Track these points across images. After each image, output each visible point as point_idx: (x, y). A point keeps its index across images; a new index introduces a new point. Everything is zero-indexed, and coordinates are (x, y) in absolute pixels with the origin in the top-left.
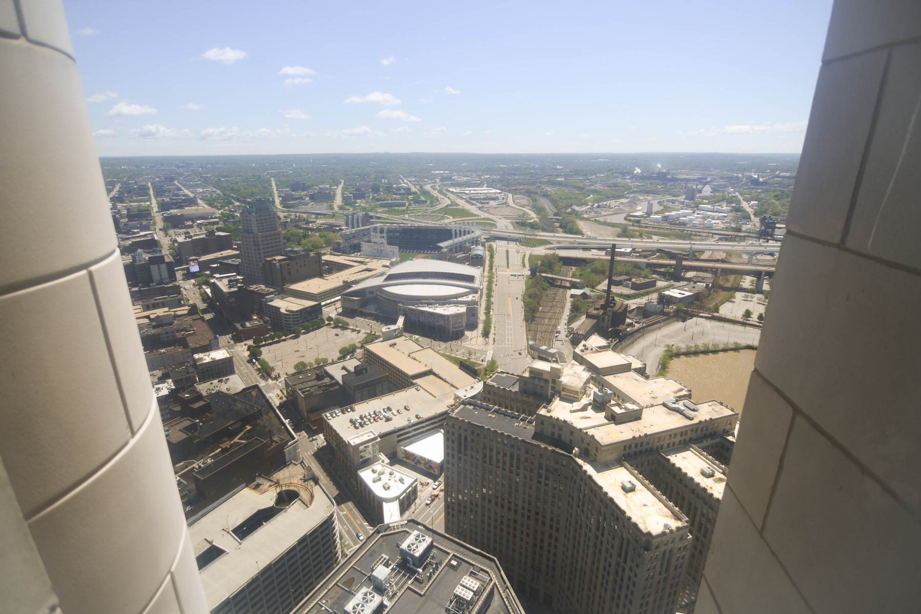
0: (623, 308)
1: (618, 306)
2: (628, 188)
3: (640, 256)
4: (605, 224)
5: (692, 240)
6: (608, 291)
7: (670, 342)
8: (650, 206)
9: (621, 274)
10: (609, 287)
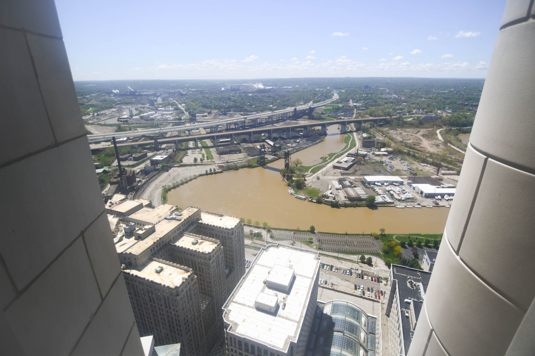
0: (132, 173)
1: (128, 173)
2: (114, 102)
3: (133, 141)
4: (105, 125)
5: (159, 127)
6: (119, 165)
7: (163, 184)
8: (131, 111)
9: (125, 154)
10: (119, 162)
